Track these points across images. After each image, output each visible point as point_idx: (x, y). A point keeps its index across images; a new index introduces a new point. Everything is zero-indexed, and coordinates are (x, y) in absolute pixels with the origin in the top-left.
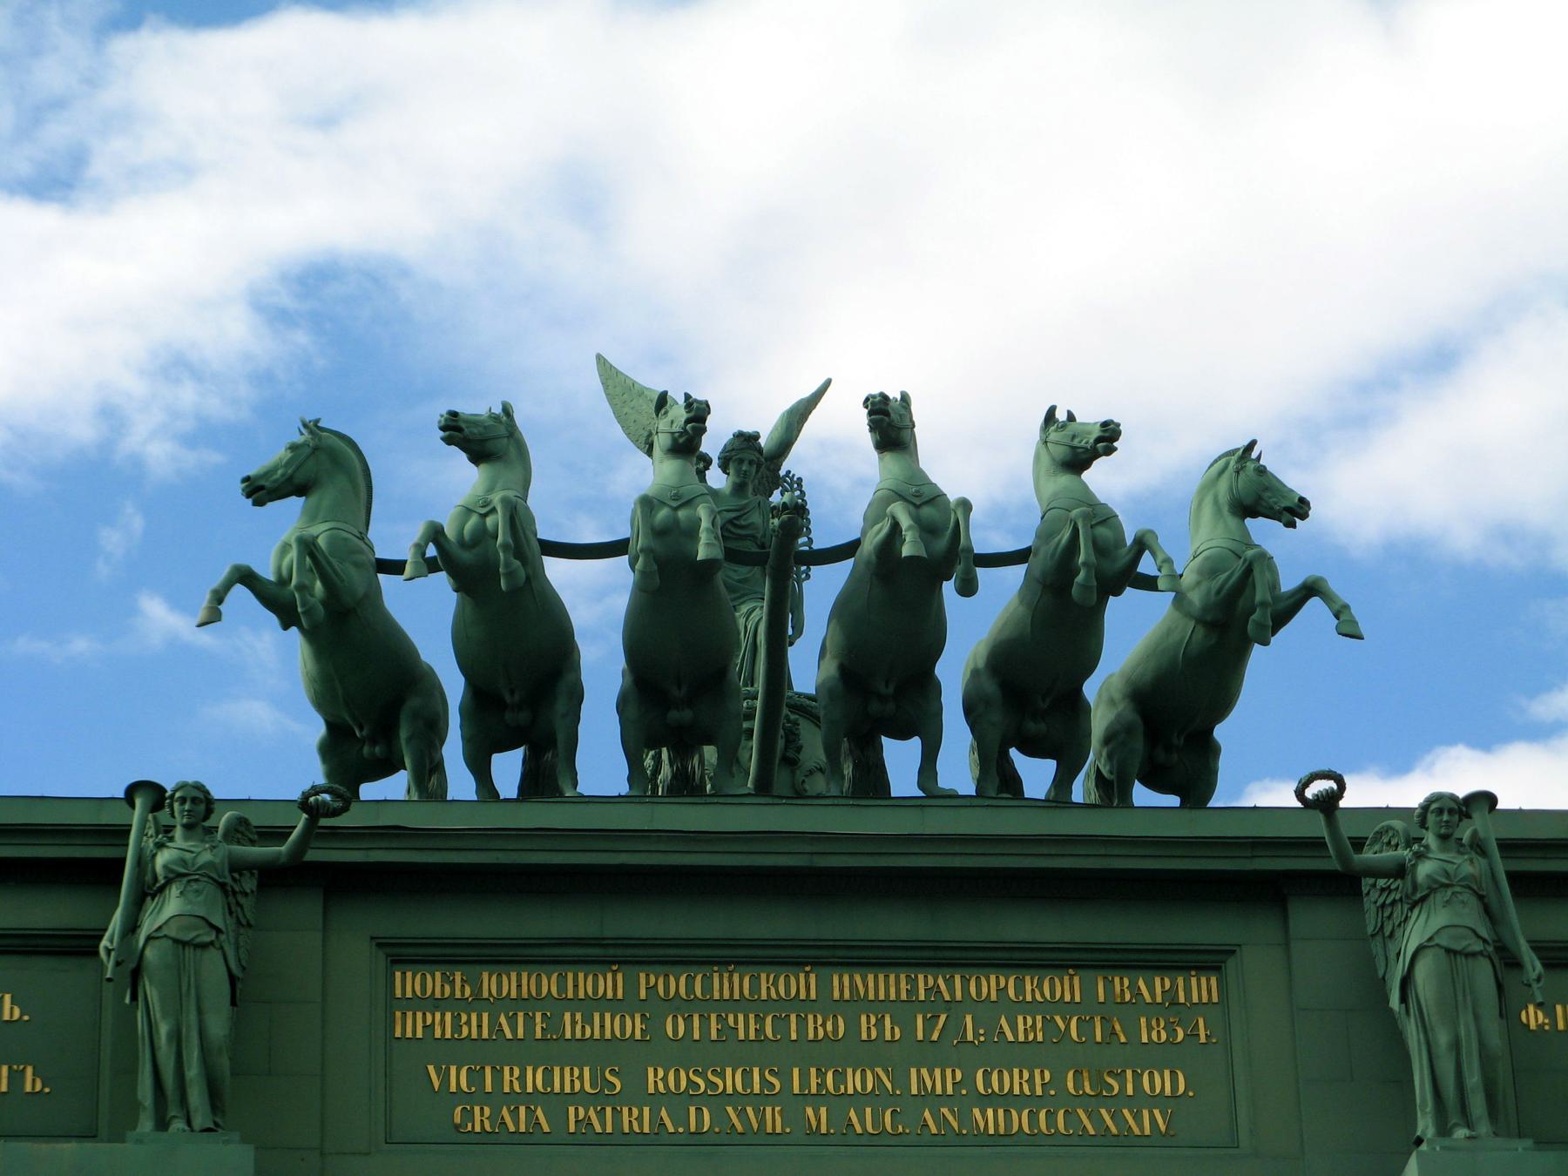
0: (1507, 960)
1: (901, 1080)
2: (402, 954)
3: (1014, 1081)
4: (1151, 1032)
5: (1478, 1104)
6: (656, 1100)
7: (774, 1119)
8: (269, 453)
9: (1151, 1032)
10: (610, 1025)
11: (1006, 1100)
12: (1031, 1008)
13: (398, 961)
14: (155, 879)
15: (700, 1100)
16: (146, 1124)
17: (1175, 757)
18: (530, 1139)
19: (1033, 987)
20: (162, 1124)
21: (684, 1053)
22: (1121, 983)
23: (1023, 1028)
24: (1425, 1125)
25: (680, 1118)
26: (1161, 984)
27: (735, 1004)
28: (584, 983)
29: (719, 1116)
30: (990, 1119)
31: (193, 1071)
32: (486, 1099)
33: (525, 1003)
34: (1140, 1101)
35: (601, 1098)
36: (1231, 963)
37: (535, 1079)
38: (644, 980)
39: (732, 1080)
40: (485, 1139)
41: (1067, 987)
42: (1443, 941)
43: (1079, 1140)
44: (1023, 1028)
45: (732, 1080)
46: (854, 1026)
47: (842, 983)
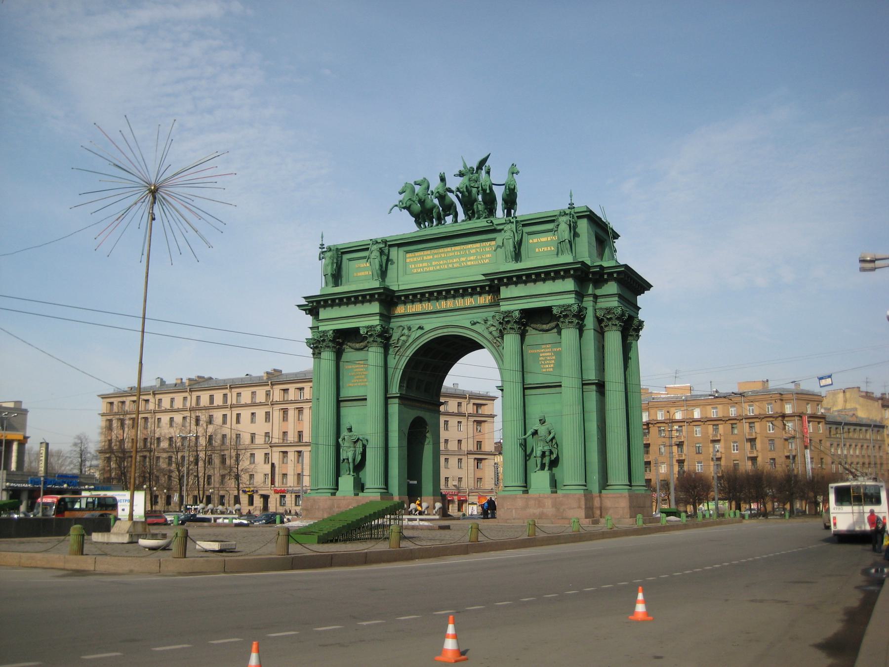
1: (460, 260)
2: (407, 252)
3: (472, 258)
4: (488, 249)
6: (434, 266)
7: (446, 267)
8: (400, 189)
9: (488, 249)
10: (429, 257)
11: (471, 260)
12: (474, 248)
13: (407, 253)
15: (438, 265)
18: (420, 273)
19: (475, 246)
21: (436, 260)
22: (484, 243)
23: (473, 251)
25: (436, 268)
26: (489, 243)
27: (442, 253)
28: (426, 252)
29: (440, 267)
30: (469, 263)
33: (420, 256)
34: (486, 258)
35: (428, 266)
36: (497, 239)
37: (421, 265)
38: (432, 251)
39: (442, 262)
40: (417, 273)
41: (478, 245)
43: (478, 265)
44: (473, 251)
45: (442, 262)
46: (454, 254)
47: (453, 248)
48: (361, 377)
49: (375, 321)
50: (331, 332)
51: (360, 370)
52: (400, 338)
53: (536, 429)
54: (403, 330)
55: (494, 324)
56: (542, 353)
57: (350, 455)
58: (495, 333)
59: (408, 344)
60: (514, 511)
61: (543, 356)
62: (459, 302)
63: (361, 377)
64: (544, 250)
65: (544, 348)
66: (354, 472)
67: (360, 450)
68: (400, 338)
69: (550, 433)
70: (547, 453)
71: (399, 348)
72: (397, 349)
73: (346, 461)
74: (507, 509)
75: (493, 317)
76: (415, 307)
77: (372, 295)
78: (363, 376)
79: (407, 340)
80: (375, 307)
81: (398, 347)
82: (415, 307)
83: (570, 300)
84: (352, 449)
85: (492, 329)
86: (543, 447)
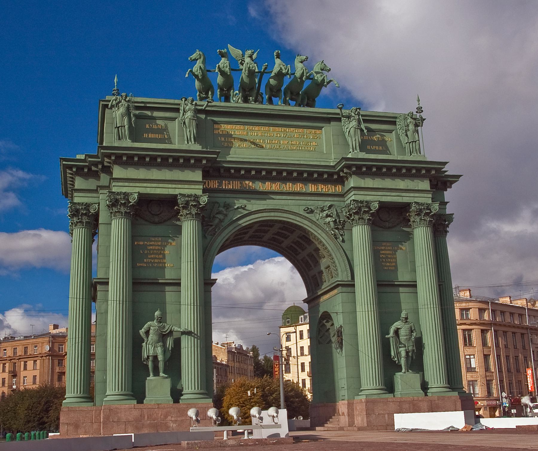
0: (362, 130)
5: (358, 148)
14: (186, 110)
16: (186, 142)
17: (310, 102)
20: (188, 143)
24: (351, 150)
31: (192, 136)
32: (226, 142)
36: (323, 129)
42: (354, 126)
48: (157, 256)
49: (197, 190)
50: (136, 196)
51: (157, 248)
52: (217, 216)
53: (399, 327)
54: (218, 207)
55: (331, 215)
56: (383, 250)
57: (159, 350)
58: (332, 224)
59: (224, 224)
60: (386, 415)
61: (383, 254)
62: (289, 187)
63: (157, 256)
64: (375, 148)
65: (385, 246)
66: (164, 372)
67: (170, 342)
68: (217, 216)
69: (412, 332)
70: (410, 354)
71: (214, 227)
72: (211, 229)
73: (151, 358)
74: (378, 414)
75: (330, 207)
76: (233, 184)
77: (198, 160)
78: (161, 256)
79: (223, 220)
80: (197, 175)
81: (212, 225)
82: (233, 184)
83: (426, 199)
84: (160, 344)
85: (329, 219)
86: (408, 347)
